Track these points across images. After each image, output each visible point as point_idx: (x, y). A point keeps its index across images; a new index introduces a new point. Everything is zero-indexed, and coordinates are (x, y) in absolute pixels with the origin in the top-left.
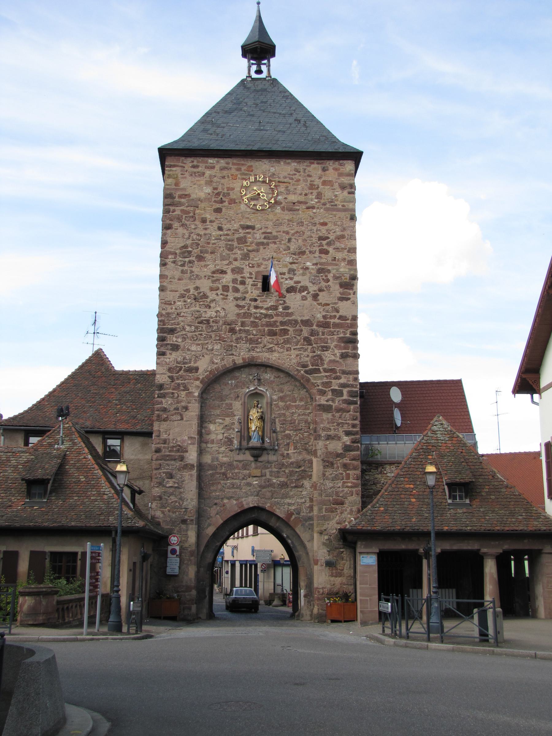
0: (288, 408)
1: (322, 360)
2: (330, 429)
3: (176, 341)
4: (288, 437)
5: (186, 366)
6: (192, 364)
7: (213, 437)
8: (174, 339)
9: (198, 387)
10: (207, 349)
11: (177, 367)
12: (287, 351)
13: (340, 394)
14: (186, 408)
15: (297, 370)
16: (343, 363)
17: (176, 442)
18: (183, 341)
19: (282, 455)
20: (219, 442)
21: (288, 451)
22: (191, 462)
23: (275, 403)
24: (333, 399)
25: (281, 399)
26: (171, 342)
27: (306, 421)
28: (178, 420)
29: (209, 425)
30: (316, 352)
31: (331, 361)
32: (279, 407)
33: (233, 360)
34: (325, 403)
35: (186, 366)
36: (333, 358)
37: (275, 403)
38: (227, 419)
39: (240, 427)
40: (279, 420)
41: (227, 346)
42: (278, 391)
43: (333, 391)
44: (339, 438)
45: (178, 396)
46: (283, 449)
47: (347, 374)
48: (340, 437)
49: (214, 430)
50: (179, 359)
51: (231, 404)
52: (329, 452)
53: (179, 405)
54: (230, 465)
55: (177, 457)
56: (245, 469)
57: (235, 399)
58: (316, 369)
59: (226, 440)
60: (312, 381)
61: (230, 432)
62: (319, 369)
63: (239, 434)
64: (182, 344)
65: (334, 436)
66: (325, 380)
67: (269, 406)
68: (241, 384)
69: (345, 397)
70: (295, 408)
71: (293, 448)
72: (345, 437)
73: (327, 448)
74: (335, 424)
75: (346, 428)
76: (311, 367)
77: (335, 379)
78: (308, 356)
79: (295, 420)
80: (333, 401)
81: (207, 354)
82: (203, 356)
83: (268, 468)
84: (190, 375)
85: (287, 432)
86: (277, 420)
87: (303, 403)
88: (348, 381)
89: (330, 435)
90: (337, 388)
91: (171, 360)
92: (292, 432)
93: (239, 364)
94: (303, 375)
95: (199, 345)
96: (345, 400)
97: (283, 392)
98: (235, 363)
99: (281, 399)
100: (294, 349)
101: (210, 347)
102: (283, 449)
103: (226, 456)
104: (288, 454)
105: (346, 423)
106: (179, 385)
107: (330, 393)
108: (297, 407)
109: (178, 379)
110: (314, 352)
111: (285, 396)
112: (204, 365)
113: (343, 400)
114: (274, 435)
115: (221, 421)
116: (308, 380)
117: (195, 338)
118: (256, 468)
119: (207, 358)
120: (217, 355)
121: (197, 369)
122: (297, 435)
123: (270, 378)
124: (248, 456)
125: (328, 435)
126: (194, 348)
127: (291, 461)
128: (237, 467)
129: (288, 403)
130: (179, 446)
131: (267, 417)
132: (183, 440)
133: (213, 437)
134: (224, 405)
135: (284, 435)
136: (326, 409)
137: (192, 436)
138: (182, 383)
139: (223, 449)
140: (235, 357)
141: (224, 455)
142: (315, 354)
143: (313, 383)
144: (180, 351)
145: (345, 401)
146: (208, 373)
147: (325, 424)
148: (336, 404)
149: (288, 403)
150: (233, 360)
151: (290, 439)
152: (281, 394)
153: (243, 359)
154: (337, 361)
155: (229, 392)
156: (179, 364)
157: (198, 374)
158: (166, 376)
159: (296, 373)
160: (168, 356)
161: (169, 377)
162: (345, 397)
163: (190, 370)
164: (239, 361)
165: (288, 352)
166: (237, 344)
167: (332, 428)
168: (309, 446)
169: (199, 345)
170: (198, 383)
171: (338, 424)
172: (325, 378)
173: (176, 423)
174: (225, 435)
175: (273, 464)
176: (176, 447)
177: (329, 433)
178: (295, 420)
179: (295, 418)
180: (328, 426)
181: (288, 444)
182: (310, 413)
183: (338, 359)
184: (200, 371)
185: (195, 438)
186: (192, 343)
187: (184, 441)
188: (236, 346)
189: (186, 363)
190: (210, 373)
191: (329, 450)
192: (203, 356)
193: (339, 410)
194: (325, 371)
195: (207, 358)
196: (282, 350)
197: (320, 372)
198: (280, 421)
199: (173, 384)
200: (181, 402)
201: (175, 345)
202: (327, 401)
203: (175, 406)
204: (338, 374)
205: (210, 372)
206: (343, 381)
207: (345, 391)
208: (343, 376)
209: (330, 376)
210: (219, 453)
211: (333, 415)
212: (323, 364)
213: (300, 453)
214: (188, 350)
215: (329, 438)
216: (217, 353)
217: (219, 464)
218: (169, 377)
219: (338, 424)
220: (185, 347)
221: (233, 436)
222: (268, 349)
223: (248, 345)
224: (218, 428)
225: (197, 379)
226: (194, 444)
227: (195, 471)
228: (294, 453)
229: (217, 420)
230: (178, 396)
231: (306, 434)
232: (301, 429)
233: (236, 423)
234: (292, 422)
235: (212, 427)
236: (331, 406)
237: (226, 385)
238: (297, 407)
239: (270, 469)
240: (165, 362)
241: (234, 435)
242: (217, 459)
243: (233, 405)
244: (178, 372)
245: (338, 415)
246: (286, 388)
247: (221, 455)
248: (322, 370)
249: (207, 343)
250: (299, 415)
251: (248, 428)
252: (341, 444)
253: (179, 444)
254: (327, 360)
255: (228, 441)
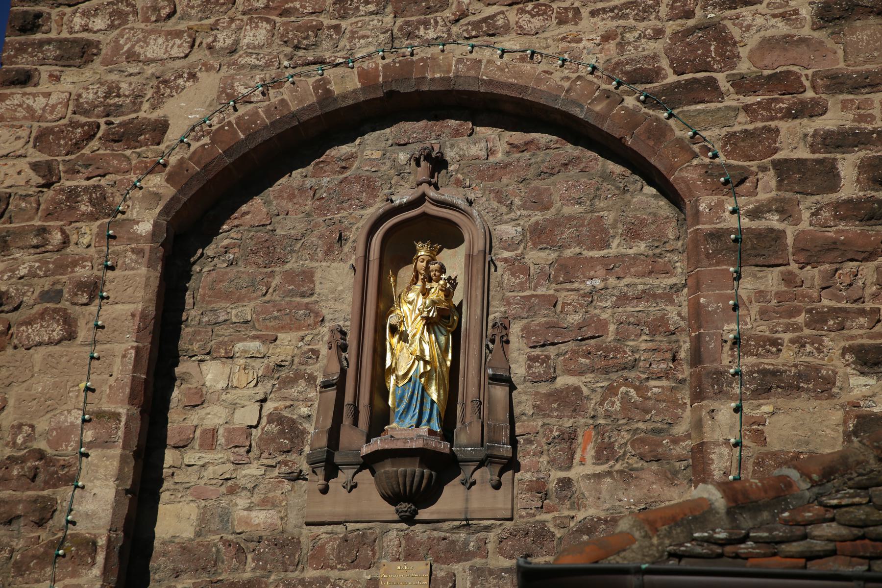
0: (566, 271)
1: (725, 41)
2: (775, 343)
3: (86, 29)
4: (570, 400)
5: (117, 121)
6: (146, 113)
7: (213, 416)
8: (78, 21)
9: (157, 196)
10: (210, 47)
11: (74, 125)
12: (561, 22)
13: (829, 177)
14: (94, 290)
15: (607, 94)
16: (830, 43)
17: (30, 438)
18: (112, 27)
19: (539, 489)
20: (242, 440)
21: (569, 468)
22: (82, 529)
23: (506, 254)
24: (782, 200)
25: (539, 235)
26: (65, 35)
27: (658, 326)
28: (50, 343)
29: (204, 366)
30: (699, 13)
31: (769, 44)
32: (526, 270)
33: (322, 84)
34: (746, 222)
35: (117, 121)
36: (782, 28)
37: (506, 254)
38: (284, 337)
39: (335, 369)
40: (525, 329)
41: (298, 29)
42: (524, 207)
43: (785, 170)
44: (825, 386)
45: (66, 242)
46: (544, 459)
47: (855, 88)
48: (830, 381)
49: (222, 384)
50: (88, 96)
51: (308, 276)
52: (775, 454)
53: (64, 278)
54: (283, 546)
55: (20, 509)
56: (353, 564)
57: (328, 252)
58: (695, 81)
59: (274, 428)
60: (678, 133)
61: (293, 392)
62: (712, 83)
63: (332, 394)
64: (106, 40)
65: (800, 376)
66: (742, 123)
67: (478, 266)
68: (357, 187)
69: (850, 187)
70: (601, 272)
71: (590, 452)
72: (863, 380)
73: (760, 437)
74: (801, 319)
75: (859, 332)
76: (672, 78)
77: (790, 114)
78: (658, 34)
79: (604, 325)
80: (785, 211)
81: (208, 68)
82: (193, 76)
83: (464, 555)
84: (128, 152)
85: (563, 381)
86: (516, 329)
87: (641, 247)
88: (861, 118)
89: (775, 373)
90: (804, 153)
91: (53, 100)
92: (589, 377)
93: (344, 97)
94: (632, 113)
95: (178, 34)
96: (849, 201)
97: (547, 208)
98: (328, 92)
99: (539, 235)
100: (593, 13)
101: (224, 39)
102: (544, 459)
103: (266, 503)
104: (566, 483)
105: (862, 312)
106: (73, 195)
107: (770, 179)
108: (610, 266)
109: (73, 172)
110: (689, 14)
111: (560, 222)
112: (188, 111)
113: (837, 206)
114: (500, 392)
115: (254, 346)
116: (659, 132)
117: (164, 12)
118: (410, 556)
119: (209, 82)
120: (255, 67)
121: (161, 128)
122: (611, 390)
123: (490, 152)
124: (367, 498)
125: (764, 372)
126: (155, 48)
127: (581, 515)
128: (318, 557)
129: (568, 253)
130: (41, 455)
131: (469, 320)
132: (59, 428)
133: (213, 416)
134: (276, 281)
135: (549, 395)
136: (751, 249)
137: (106, 407)
138: (86, 189)
139: (254, 470)
140: (330, 73)
141: (256, 498)
142: (691, 23)
143: (680, 141)
144: (97, 64)
145: (849, 210)
146: (206, 140)
147: (753, 323)
148: (804, 225)
149: (568, 253)
150: (322, 84)
151: (576, 410)
152: (538, 217)
153: (363, 75)
154: (803, 41)
155: (301, 227)
156: (86, 113)
157: (162, 147)
158: (23, 164)
159: (598, 108)
160: (45, 86)
161: (35, 166)
162: (850, 187)
163: (128, 136)
164: (345, 83)
165: (565, 29)
166: (343, 18)
167: (787, 337)
168: (675, 441)
169: (178, 34)
170: (156, 182)
171: (818, 319)
172: (742, 117)
173: (38, 355)
174: (269, 407)
175: (492, 536)
176: (23, 460)
177: (768, 362)
178: (604, 325)
179: (604, 316)
180: (763, 329)
181: (569, 438)
182: (676, 289)
183: (806, 32)
184: (173, 135)
185: (116, 416)
186: (152, 31)
187: (63, 433)
188: (337, 28)
189: (118, 109)
190: (213, 141)
191: (775, 444)
192: (193, 76)
193: (813, 252)
194: (741, 84)
195: (209, 82)
196: (537, 22)
197: (720, 95)
198: (527, 332)
199: (49, 193)
200: (75, 264)
201: (75, 41)
202: (755, 214)
203: (46, 284)
204: (810, 94)
205: (216, 137)
206: (832, 120)
207: (848, 166)
208: (833, 102)
209: (766, 106)
210: (232, 491)
211: (789, 279)
212: (729, 59)
213: (628, 476)
214: (132, 57)
215: (768, 383)
216: (252, 60)
217: (228, 544)
218: (35, 167)
219: (818, 319)
220: (117, 47)
221: (304, 411)
222: (476, 25)
223: (388, 19)
224: (241, 378)
225: (157, 167)
226: (104, 443)
227: (96, 571)
228: (598, 476)
229: (239, 346)
230: (66, 242)
231: (655, 387)
232: (634, 365)
233: (324, 351)
234: (588, 334)
235: (213, 374)
236: (778, 236)
237: (291, 197)
238: (610, 266)
239: (478, 561)
240: (29, 108)
241: (310, 408)
242: (225, 517)
243: (317, 277)
244: (77, 146)
245: (813, 275)
246: (559, 188)
247: (242, 502)
248: (724, 84)
249: (213, 28)
250: (623, 299)
251: (381, 373)
252: (838, 415)
253: (42, 445)
254: (753, 40)
255: (282, 432)
